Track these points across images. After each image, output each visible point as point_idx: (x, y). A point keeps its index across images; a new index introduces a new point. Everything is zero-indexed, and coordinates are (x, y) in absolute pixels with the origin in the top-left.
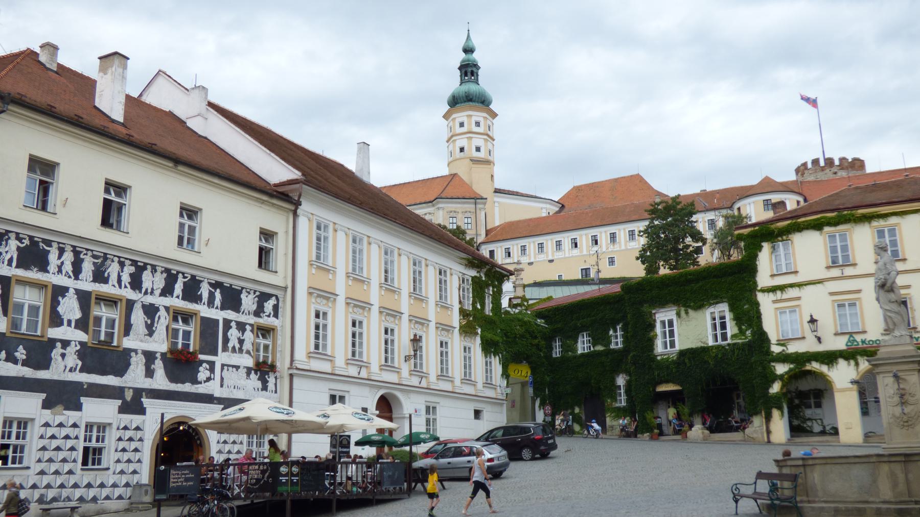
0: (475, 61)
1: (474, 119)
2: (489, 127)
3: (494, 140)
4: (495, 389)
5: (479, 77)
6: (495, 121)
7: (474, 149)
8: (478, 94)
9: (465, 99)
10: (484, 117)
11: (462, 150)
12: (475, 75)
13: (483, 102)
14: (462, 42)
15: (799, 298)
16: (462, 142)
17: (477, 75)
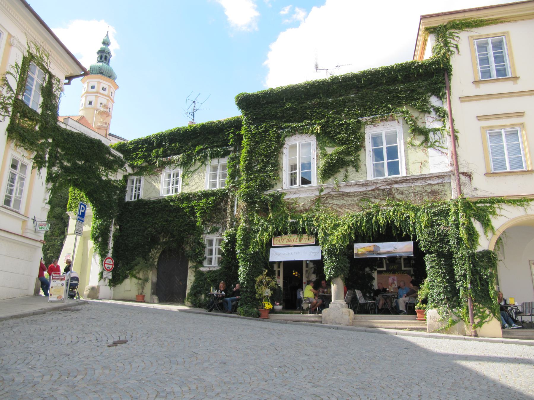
0: (109, 50)
1: (102, 85)
2: (112, 94)
3: (113, 102)
4: (24, 221)
5: (110, 62)
6: (117, 92)
7: (99, 104)
8: (107, 71)
9: (98, 72)
10: (109, 86)
11: (90, 103)
12: (108, 59)
13: (110, 77)
14: (103, 37)
15: (521, 114)
16: (92, 98)
17: (109, 60)
